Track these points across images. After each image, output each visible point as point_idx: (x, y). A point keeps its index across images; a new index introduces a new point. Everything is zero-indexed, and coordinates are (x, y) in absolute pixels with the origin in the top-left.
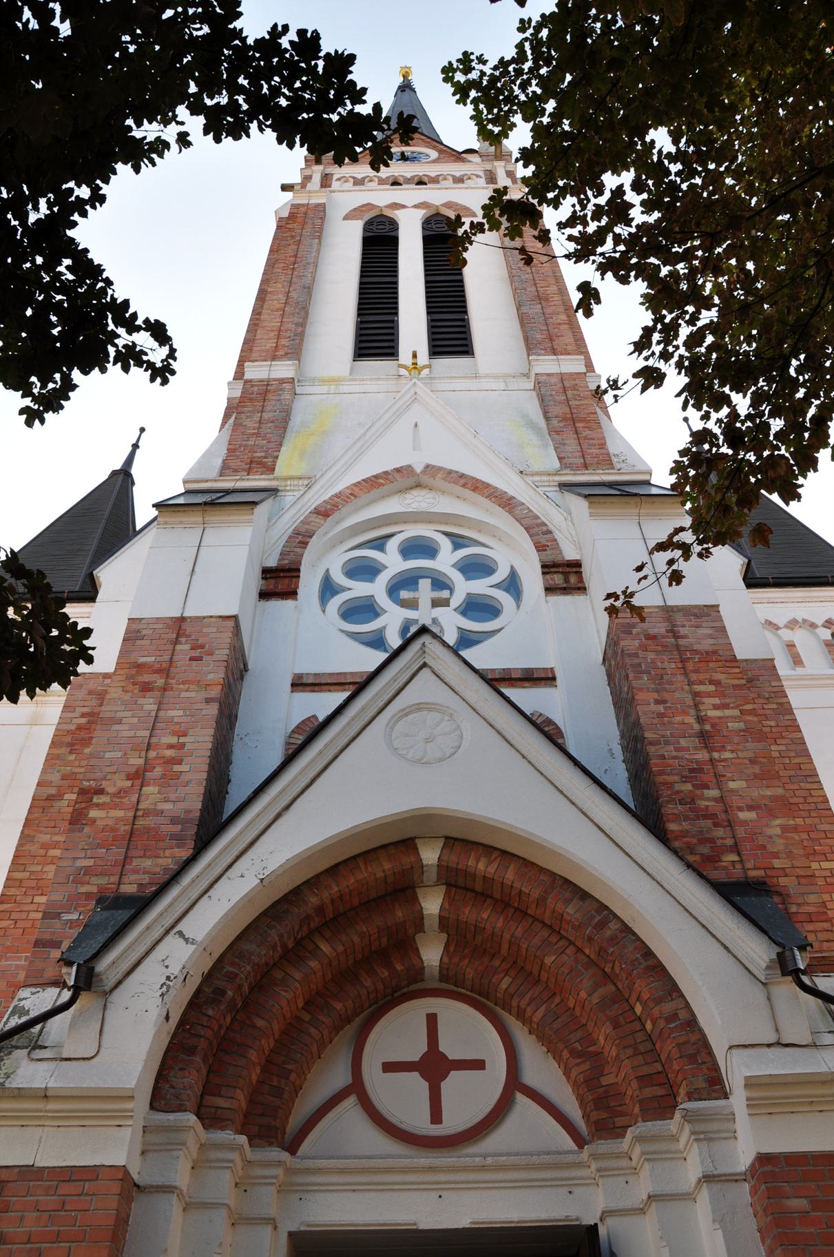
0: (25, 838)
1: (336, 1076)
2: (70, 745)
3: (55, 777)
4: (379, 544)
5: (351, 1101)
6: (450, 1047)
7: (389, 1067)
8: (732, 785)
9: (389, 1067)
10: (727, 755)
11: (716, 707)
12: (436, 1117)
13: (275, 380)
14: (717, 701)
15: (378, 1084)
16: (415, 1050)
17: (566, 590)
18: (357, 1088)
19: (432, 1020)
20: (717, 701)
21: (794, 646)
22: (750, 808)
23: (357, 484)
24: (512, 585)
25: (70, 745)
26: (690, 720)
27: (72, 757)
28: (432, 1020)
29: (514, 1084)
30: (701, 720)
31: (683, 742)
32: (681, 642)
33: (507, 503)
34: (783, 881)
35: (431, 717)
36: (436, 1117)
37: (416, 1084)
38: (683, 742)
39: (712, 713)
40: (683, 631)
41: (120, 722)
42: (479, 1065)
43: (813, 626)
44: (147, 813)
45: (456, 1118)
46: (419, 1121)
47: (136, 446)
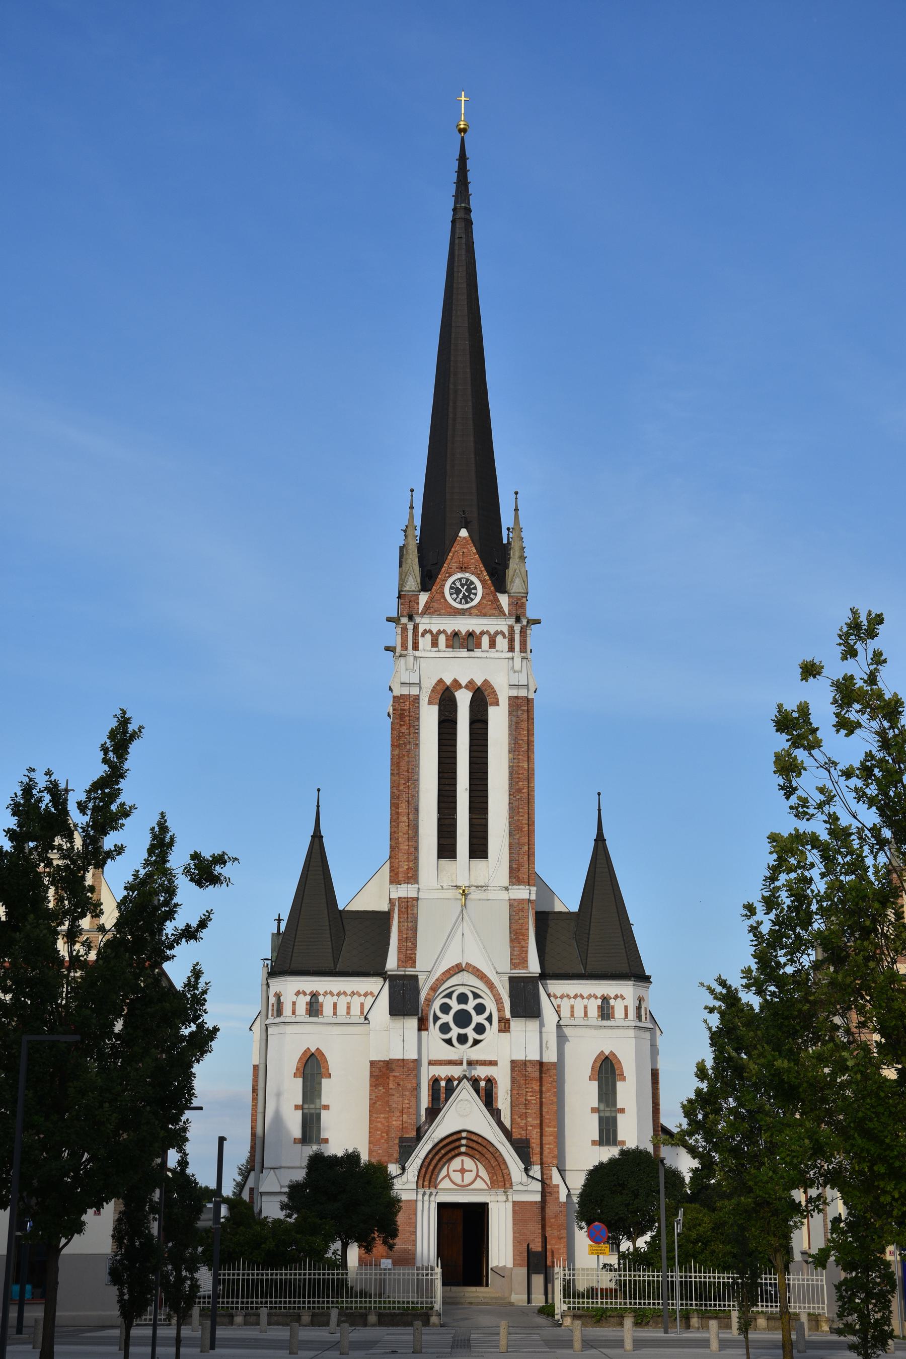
0: (371, 1116)
1: (444, 1173)
2: (375, 1086)
3: (373, 1097)
4: (449, 996)
5: (447, 1179)
6: (466, 1167)
7: (454, 1171)
8: (529, 1120)
9: (454, 1171)
10: (530, 1111)
11: (531, 1096)
12: (463, 1181)
13: (411, 898)
14: (531, 1094)
15: (452, 1174)
16: (459, 1168)
17: (504, 1032)
18: (448, 1175)
19: (462, 1160)
20: (531, 1094)
21: (587, 1007)
22: (531, 1126)
23: (443, 974)
24: (489, 1019)
25: (375, 1086)
26: (524, 1100)
27: (376, 1090)
28: (462, 1160)
29: (477, 1176)
30: (526, 1100)
31: (520, 1107)
32: (527, 1073)
33: (491, 986)
34: (533, 1145)
35: (466, 1102)
36: (463, 1181)
37: (459, 1174)
38: (520, 1107)
39: (529, 1098)
40: (528, 1069)
41: (394, 1095)
42: (471, 1171)
43: (596, 998)
44: (405, 1122)
45: (466, 1182)
46: (459, 1181)
47: (318, 806)
